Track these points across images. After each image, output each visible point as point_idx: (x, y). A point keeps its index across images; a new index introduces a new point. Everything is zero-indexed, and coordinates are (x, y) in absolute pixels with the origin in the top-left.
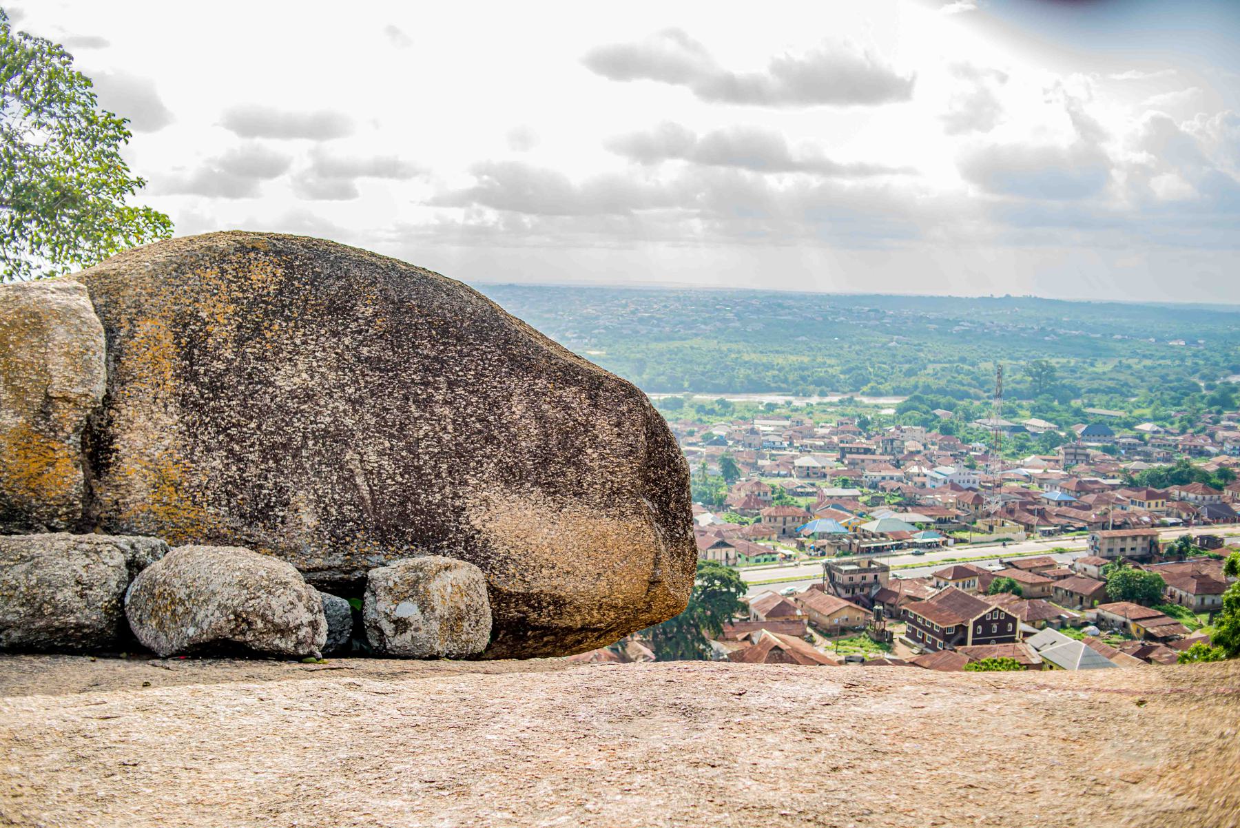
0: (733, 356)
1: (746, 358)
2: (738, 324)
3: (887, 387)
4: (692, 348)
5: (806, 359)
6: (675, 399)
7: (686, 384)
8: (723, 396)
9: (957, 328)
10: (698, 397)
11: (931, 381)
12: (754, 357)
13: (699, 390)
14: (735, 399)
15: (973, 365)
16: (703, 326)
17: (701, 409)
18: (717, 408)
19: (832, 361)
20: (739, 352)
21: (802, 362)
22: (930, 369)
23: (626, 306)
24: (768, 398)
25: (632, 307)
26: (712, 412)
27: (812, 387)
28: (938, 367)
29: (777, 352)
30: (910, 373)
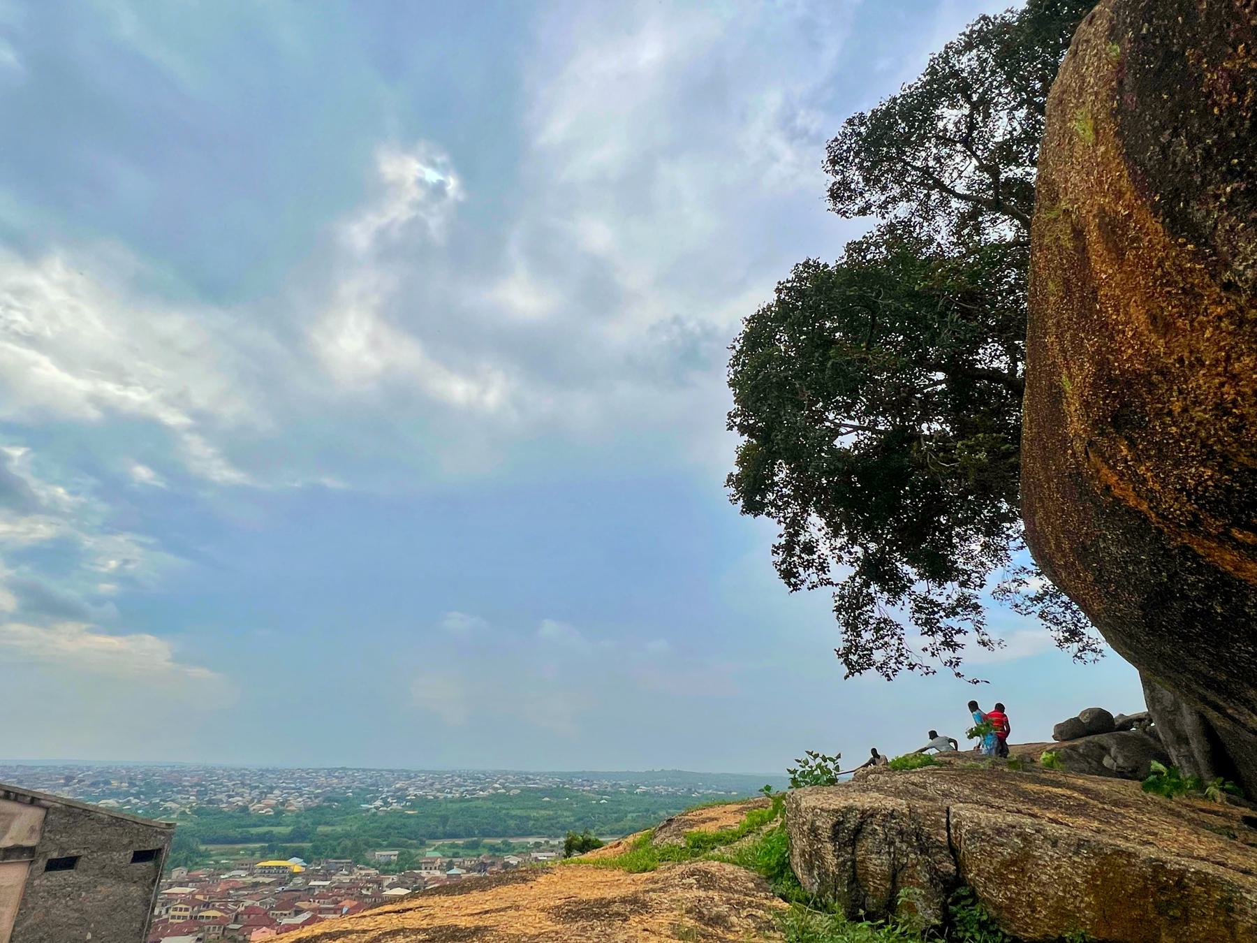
0: (504, 812)
1: (514, 813)
2: (503, 791)
3: (607, 828)
4: (476, 807)
5: (551, 813)
6: (474, 842)
7: (476, 832)
8: (506, 839)
9: (638, 790)
10: (487, 841)
11: (633, 824)
12: (518, 812)
13: (489, 836)
14: (511, 841)
15: (654, 813)
16: (481, 793)
17: (493, 848)
18: (501, 846)
19: (568, 814)
20: (507, 809)
21: (549, 815)
22: (629, 816)
23: (425, 781)
24: (532, 840)
25: (430, 781)
26: (498, 850)
27: (559, 831)
28: (635, 815)
29: (532, 808)
30: (617, 820)
